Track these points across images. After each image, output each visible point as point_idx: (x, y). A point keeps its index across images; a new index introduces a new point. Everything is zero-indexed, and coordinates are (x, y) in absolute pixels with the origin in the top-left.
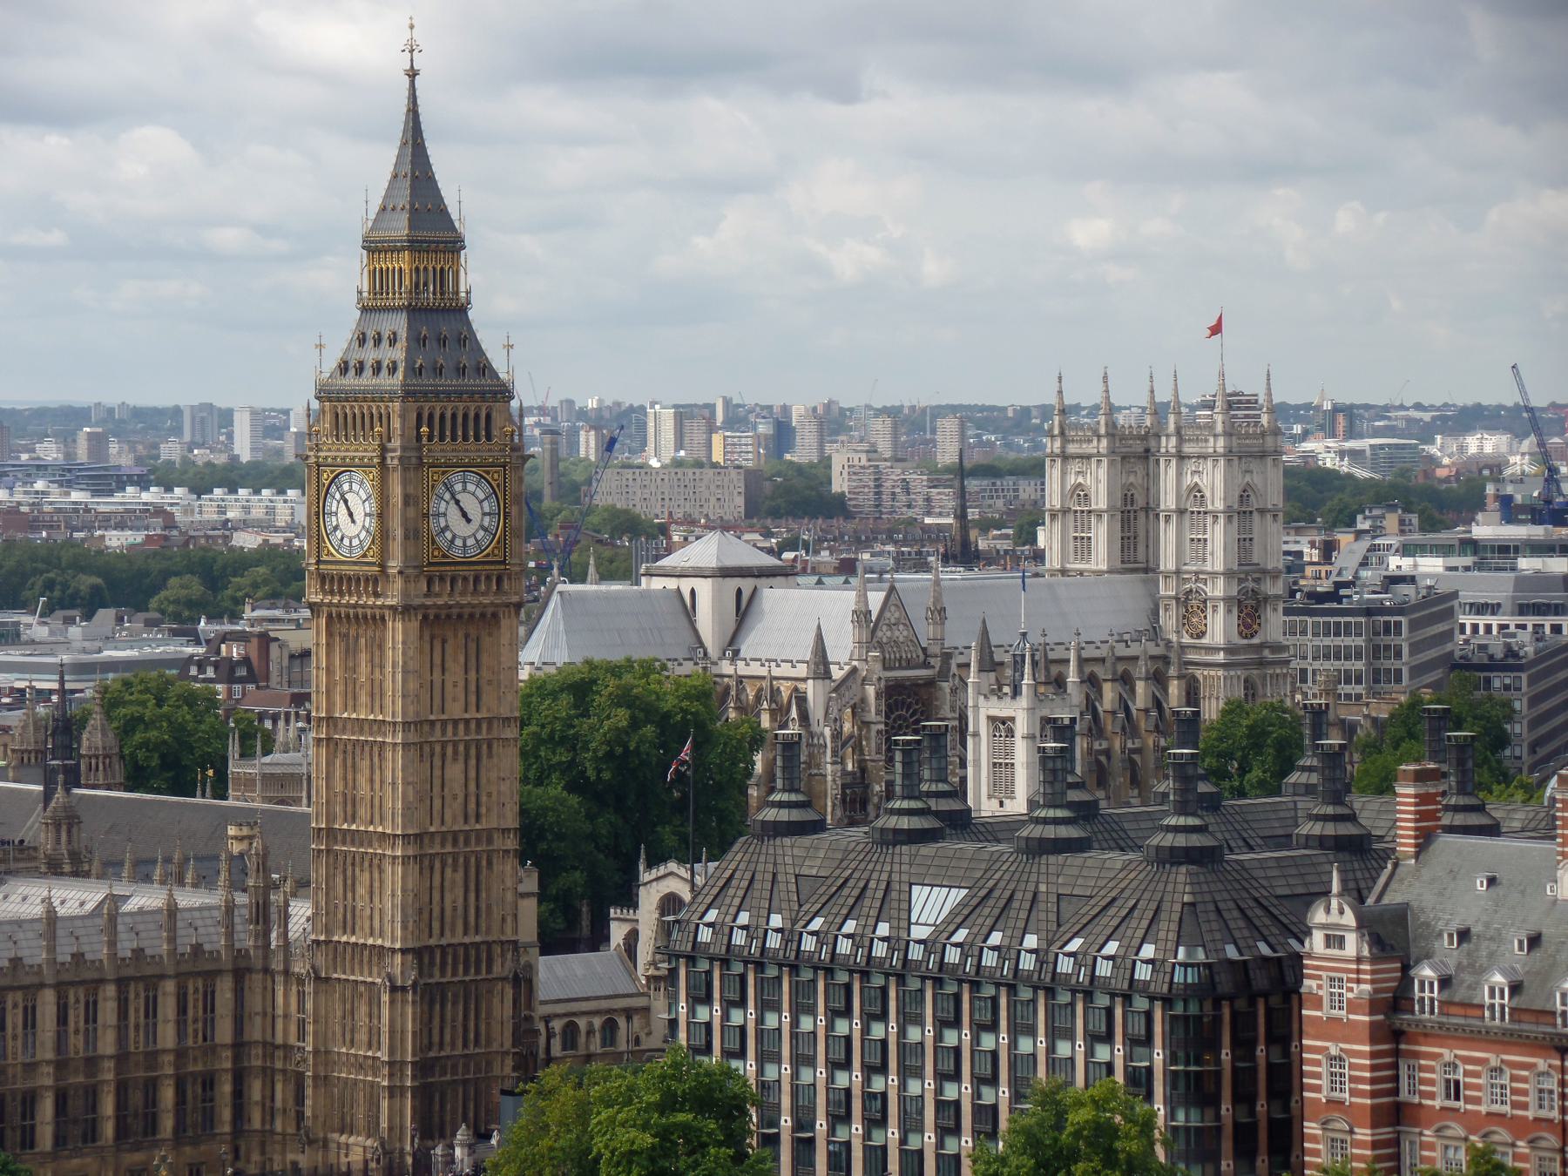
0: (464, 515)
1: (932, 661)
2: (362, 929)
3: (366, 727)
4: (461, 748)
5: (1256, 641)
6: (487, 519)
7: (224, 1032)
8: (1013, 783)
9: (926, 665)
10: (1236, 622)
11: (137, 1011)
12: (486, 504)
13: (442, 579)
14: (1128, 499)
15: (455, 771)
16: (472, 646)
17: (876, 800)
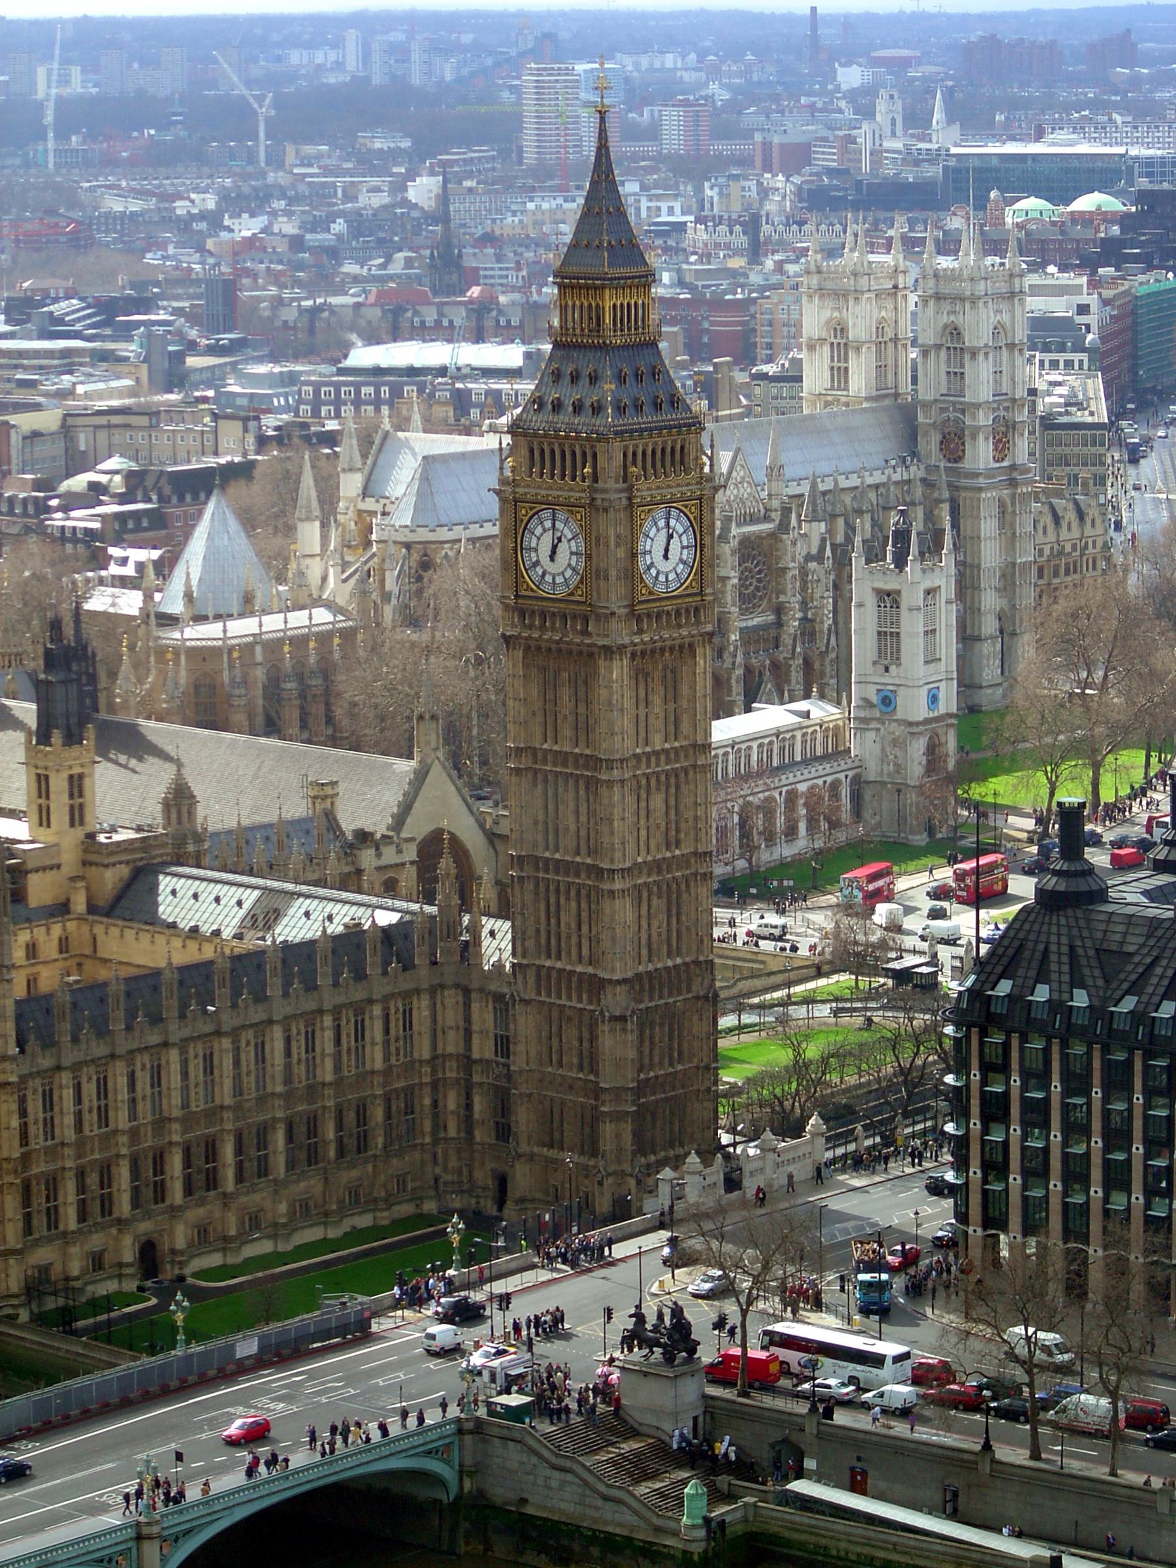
0: (667, 550)
1: (773, 515)
2: (569, 954)
3: (571, 761)
4: (663, 778)
5: (1006, 463)
6: (685, 552)
7: (423, 1050)
8: (898, 651)
9: (767, 519)
10: (991, 447)
11: (348, 1036)
12: (684, 537)
13: (649, 616)
14: (880, 330)
15: (657, 801)
16: (669, 676)
17: (732, 648)
